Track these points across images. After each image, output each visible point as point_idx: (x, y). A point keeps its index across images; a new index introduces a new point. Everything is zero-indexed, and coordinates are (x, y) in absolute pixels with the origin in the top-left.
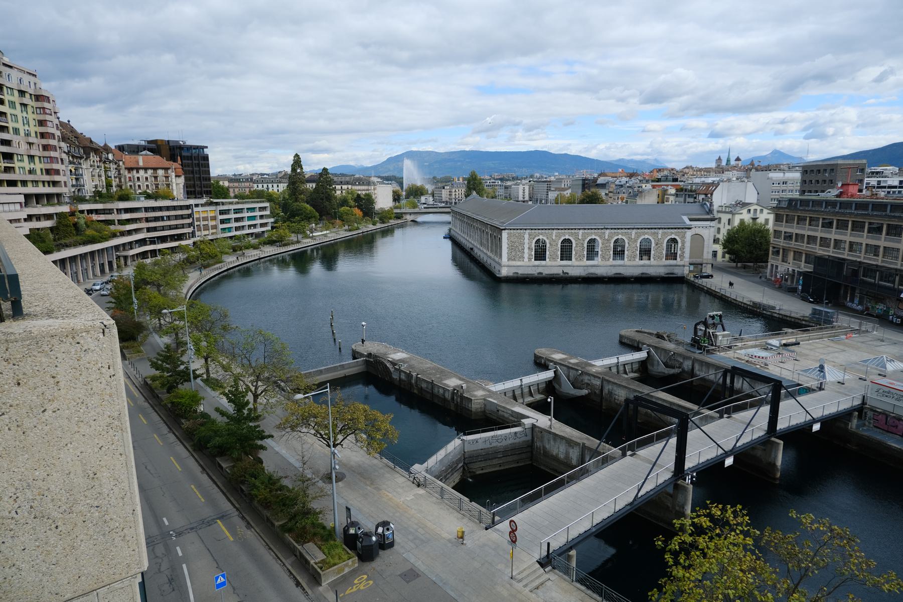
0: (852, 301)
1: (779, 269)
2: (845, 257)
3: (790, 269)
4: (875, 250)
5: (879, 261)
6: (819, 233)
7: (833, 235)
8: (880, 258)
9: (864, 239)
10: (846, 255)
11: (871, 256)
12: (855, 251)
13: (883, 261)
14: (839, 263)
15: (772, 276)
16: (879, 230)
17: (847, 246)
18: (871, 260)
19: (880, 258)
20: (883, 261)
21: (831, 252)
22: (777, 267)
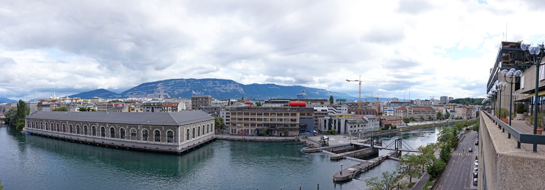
0: (275, 133)
1: (237, 130)
2: (270, 123)
3: (243, 129)
4: (281, 120)
5: (283, 122)
6: (256, 117)
7: (263, 117)
8: (283, 121)
9: (276, 117)
10: (270, 122)
11: (279, 121)
12: (273, 121)
13: (284, 122)
14: (267, 125)
15: (233, 133)
16: (282, 115)
17: (270, 120)
18: (280, 122)
19: (283, 121)
20: (284, 122)
21: (263, 122)
22: (235, 130)
